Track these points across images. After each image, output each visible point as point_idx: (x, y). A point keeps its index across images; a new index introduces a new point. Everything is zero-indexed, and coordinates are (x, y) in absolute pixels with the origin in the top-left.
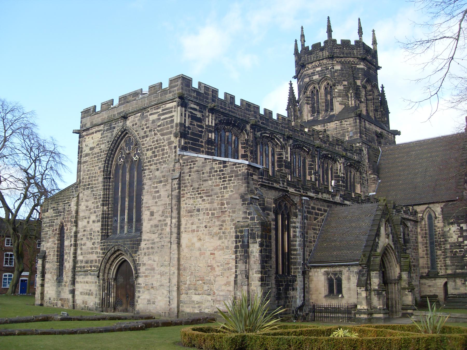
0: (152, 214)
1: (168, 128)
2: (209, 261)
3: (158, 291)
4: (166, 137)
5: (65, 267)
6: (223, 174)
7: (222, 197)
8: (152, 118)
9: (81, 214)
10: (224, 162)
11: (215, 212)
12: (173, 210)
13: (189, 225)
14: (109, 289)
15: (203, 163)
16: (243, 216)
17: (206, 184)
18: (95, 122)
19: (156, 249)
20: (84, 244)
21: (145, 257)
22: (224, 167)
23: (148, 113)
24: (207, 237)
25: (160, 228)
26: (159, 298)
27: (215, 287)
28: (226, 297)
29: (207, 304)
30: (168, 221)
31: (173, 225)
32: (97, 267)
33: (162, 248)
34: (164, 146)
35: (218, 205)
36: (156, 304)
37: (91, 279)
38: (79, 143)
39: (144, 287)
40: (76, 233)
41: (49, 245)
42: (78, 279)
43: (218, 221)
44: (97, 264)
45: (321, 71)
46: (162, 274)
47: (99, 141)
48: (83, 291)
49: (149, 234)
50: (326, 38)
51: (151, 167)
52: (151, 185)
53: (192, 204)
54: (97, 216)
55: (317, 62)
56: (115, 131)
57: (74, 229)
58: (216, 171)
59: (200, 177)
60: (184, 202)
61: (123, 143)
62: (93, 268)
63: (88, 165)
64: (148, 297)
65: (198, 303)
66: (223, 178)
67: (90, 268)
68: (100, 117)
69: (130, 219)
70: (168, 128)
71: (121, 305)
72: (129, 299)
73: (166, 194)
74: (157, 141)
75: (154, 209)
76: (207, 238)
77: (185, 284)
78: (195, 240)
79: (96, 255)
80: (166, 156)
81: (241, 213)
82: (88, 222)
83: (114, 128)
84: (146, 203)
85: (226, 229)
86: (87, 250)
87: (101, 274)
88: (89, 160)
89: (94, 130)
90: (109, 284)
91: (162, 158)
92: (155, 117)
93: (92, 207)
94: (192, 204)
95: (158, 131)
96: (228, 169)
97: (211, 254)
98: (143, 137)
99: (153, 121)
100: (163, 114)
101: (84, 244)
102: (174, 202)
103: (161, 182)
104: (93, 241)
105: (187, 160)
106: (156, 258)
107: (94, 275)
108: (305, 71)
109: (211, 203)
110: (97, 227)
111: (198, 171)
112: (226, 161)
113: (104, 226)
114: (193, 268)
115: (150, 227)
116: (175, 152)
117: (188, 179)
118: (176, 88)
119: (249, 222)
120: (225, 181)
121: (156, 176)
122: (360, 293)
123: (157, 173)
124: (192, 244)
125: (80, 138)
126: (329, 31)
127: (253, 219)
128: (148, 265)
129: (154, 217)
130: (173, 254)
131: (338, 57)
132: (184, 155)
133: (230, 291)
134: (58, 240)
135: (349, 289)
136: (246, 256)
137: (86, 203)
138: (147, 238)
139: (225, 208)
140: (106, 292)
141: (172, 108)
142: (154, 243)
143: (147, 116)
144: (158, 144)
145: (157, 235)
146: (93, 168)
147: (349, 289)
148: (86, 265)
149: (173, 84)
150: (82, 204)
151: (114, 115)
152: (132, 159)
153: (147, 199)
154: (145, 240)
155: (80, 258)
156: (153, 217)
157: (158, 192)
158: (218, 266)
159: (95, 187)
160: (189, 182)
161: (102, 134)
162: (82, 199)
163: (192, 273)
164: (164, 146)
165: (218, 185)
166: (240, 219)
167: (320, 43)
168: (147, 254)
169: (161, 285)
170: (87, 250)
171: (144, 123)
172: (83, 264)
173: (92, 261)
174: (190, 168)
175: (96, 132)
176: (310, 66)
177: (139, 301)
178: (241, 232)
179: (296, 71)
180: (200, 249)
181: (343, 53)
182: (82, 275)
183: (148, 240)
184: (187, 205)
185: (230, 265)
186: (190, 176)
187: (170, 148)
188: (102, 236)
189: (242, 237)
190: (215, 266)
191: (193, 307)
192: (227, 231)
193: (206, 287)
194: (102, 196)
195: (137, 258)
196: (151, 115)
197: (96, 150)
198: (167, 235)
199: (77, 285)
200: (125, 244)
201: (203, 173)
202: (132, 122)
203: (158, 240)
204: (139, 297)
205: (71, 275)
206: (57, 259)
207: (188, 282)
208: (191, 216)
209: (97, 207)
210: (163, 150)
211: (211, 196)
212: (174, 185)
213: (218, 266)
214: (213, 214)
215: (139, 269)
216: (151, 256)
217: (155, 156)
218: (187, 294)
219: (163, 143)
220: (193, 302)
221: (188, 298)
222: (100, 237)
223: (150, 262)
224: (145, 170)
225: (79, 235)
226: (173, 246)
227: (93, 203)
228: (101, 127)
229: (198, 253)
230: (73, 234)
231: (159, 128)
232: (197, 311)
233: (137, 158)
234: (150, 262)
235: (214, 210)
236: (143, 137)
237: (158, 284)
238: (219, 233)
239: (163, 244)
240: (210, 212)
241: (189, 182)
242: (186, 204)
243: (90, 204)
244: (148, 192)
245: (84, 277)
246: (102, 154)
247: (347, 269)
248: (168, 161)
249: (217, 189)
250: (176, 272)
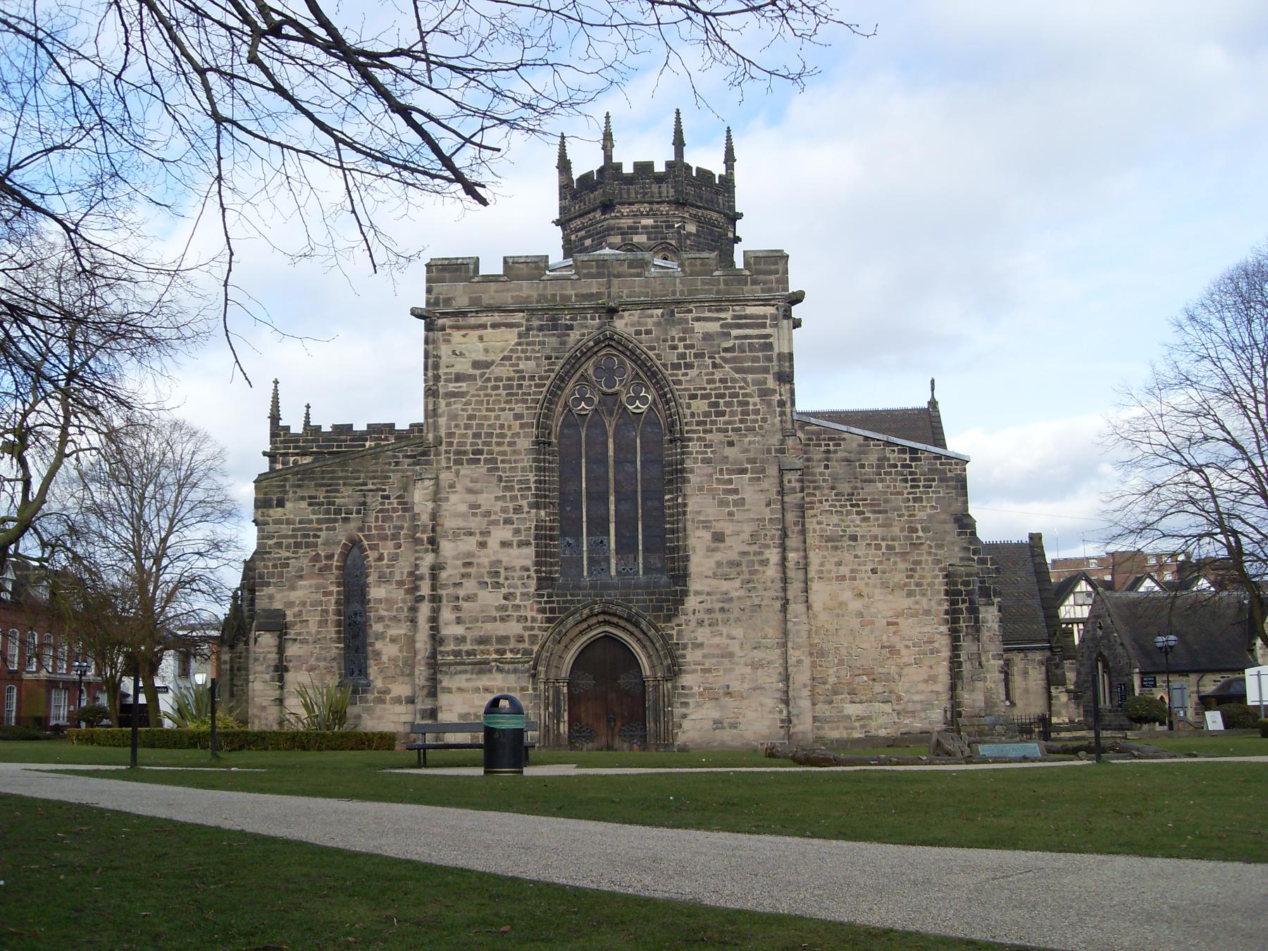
0: (719, 537)
1: (755, 359)
2: (885, 637)
3: (745, 702)
4: (750, 377)
5: (378, 654)
6: (911, 473)
7: (910, 516)
8: (700, 327)
9: (449, 523)
10: (914, 451)
11: (896, 543)
12: (790, 534)
13: (828, 567)
14: (557, 706)
15: (859, 445)
16: (961, 555)
17: (869, 488)
18: (486, 300)
19: (736, 613)
20: (468, 598)
21: (700, 630)
22: (912, 459)
23: (690, 316)
24: (877, 591)
25: (744, 568)
26: (750, 715)
27: (900, 688)
28: (928, 705)
29: (881, 720)
30: (773, 556)
31: (790, 565)
32: (527, 652)
33: (752, 611)
34: (750, 395)
35: (902, 530)
36: (742, 727)
37: (504, 680)
38: (427, 342)
39: (701, 694)
40: (436, 569)
41: (295, 595)
42: (446, 682)
43: (905, 561)
44: (526, 645)
45: (653, 227)
46: (756, 666)
47: (511, 351)
48: (472, 711)
49: (714, 582)
50: (671, 157)
51: (708, 436)
52: (711, 475)
53: (835, 525)
54: (517, 531)
56: (574, 336)
57: (429, 559)
58: (896, 466)
59: (855, 473)
60: (814, 520)
61: (589, 367)
62: (509, 655)
63: (467, 403)
64: (716, 715)
65: (859, 718)
66: (912, 480)
67: (495, 656)
68: (508, 290)
69: (626, 546)
70: (755, 359)
71: (591, 737)
72: (619, 724)
73: (762, 498)
74: (722, 381)
75: (728, 528)
76: (878, 593)
77: (824, 683)
78: (847, 595)
79: (521, 625)
80: (752, 417)
81: (957, 549)
82: (483, 545)
83: (571, 328)
84: (699, 513)
85: (922, 577)
86: (482, 611)
87: (541, 669)
88: (474, 392)
89: (484, 319)
90: (557, 692)
91: (741, 421)
92: (714, 327)
93: (497, 509)
94: (835, 525)
95: (725, 360)
96: (924, 465)
97: (889, 624)
98: (676, 367)
99: (707, 337)
100: (739, 326)
101: (468, 598)
102: (791, 517)
103: (744, 471)
104: (504, 591)
105: (818, 434)
106: (738, 632)
107: (515, 671)
108: (612, 218)
109: (886, 525)
110: (526, 557)
111: (848, 460)
112: (917, 450)
113: (542, 557)
114: (843, 652)
115: (713, 565)
116: (782, 414)
117: (821, 474)
118: (773, 277)
119: (976, 567)
120: (918, 487)
121: (727, 457)
122: (1057, 697)
123: (728, 451)
124: (841, 604)
125: (429, 328)
126: (679, 143)
127: (982, 561)
128: (712, 645)
129: (728, 543)
130: (795, 623)
131: (693, 205)
132: (810, 424)
133: (938, 693)
134: (339, 585)
135: (1027, 691)
136: (976, 628)
137: (471, 498)
138: (706, 589)
139: (918, 537)
140: (551, 709)
141: (765, 317)
142: (730, 600)
143: (686, 321)
144: (726, 388)
145: (737, 583)
146: (493, 414)
147: (1027, 691)
148: (482, 647)
149: (762, 267)
150: (453, 498)
151: (566, 298)
152: (625, 409)
153: (699, 502)
154: (697, 593)
155: (451, 630)
156: (721, 545)
157: (736, 491)
158: (907, 647)
159: (503, 461)
160: (824, 480)
161: (520, 336)
162: (452, 486)
163: (841, 662)
164: (745, 395)
165: (901, 493)
166: (956, 561)
167: (651, 165)
168: (706, 622)
169: (755, 689)
170: (482, 611)
171: (675, 332)
172: (465, 647)
173: (503, 639)
174: (828, 452)
175: (494, 326)
176: (625, 210)
177: (686, 724)
178: (966, 584)
179: (563, 210)
180: (860, 615)
181: (701, 198)
182: (466, 672)
183: (708, 594)
184: (824, 526)
185: (936, 645)
186: (826, 467)
187: (769, 404)
188: (539, 579)
189: (969, 593)
190: (899, 646)
191: (846, 728)
192: (925, 582)
193: (878, 688)
194: (533, 486)
195: (674, 632)
196: (698, 319)
197: (497, 371)
198: (769, 584)
199: (443, 699)
200: (630, 601)
201: (862, 466)
202: (633, 325)
203: (741, 593)
204: (685, 716)
205: (425, 674)
206: (338, 632)
207: (832, 680)
208: (836, 548)
209: (518, 510)
210: (747, 403)
211: (886, 512)
212: (790, 481)
213: (907, 647)
214: (889, 547)
215: (684, 656)
216: (719, 628)
217: (723, 414)
218: (831, 702)
219: (741, 388)
220: (849, 717)
221: (834, 711)
222: (533, 584)
223: (716, 640)
224: (690, 440)
225: (443, 575)
226: (792, 607)
227: (497, 498)
228: (519, 317)
229: (855, 622)
230: (424, 570)
231: (728, 355)
232: (857, 735)
233: (638, 407)
234: (716, 640)
235: (893, 540)
236: (676, 367)
237: (746, 686)
238: (906, 585)
239: (757, 601)
240: (884, 544)
241: (824, 480)
242: (819, 523)
243: (486, 500)
244: (701, 489)
245: (474, 676)
246: (526, 383)
247: (1022, 655)
248: (761, 428)
249: (898, 501)
250: (807, 661)
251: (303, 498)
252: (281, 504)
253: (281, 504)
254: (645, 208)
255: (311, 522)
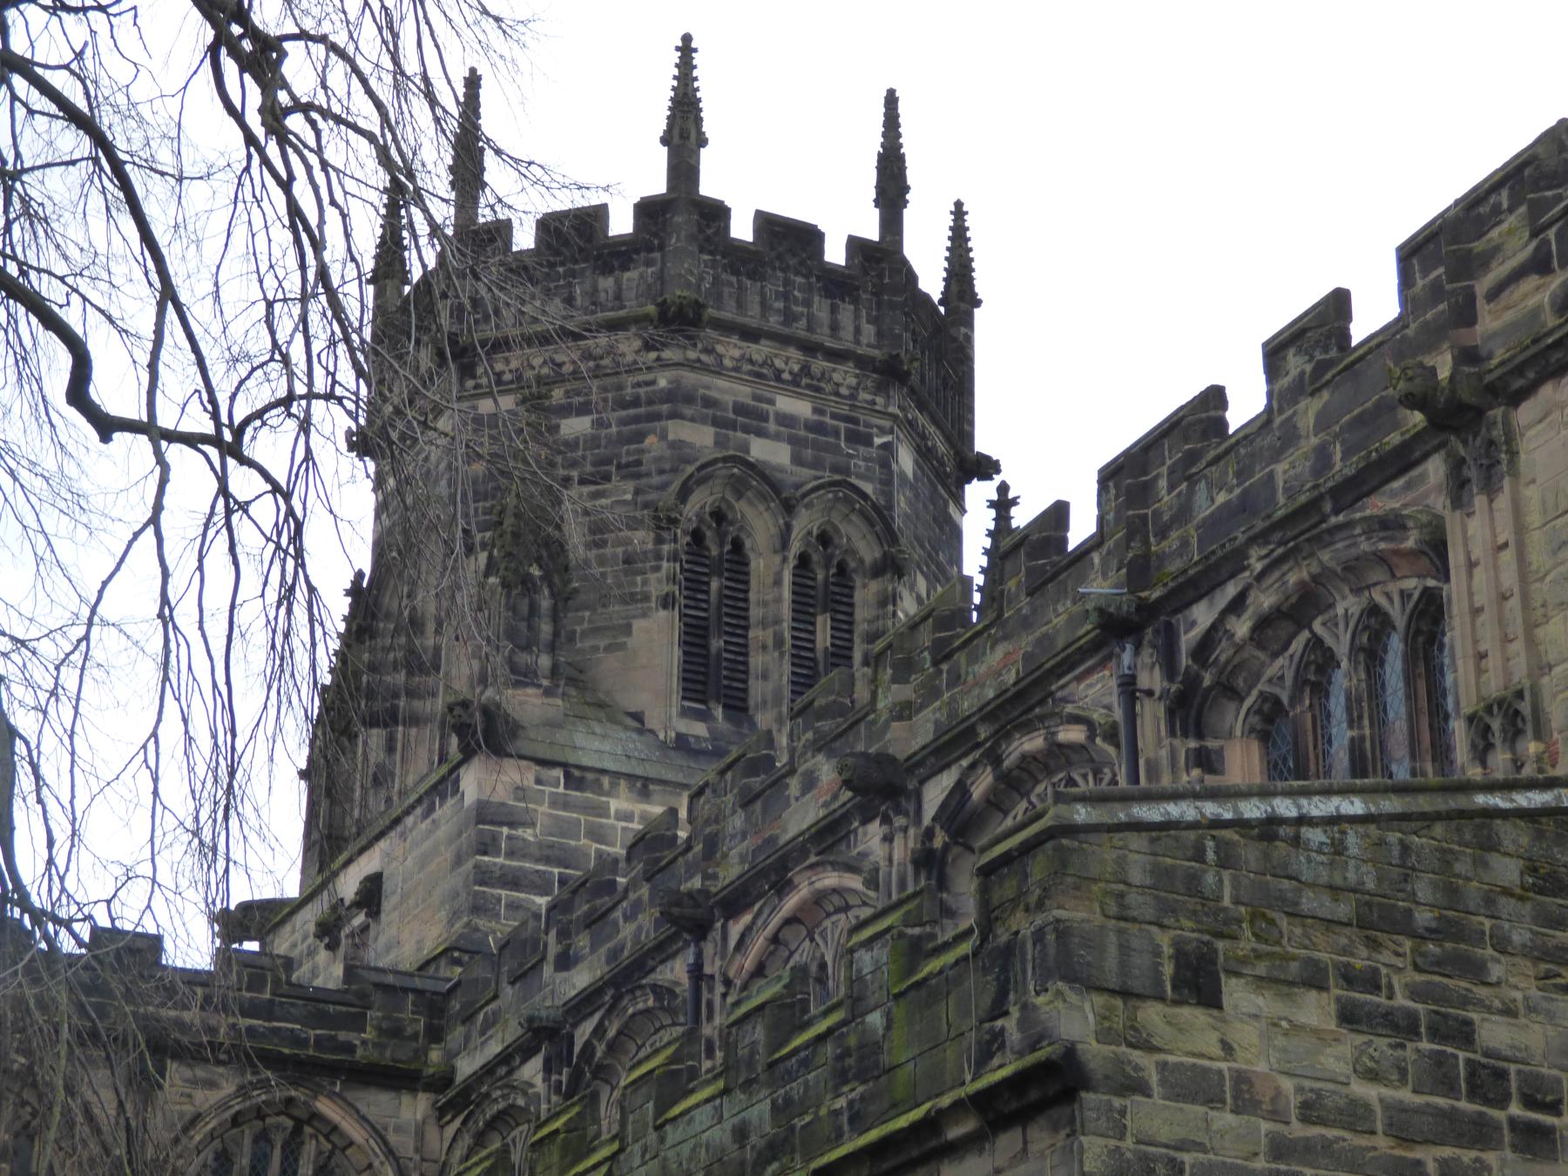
55: (793, 353)
176: (731, 349)
251: (1314, 979)
252: (1199, 982)
253: (1199, 982)
254: (790, 360)
255: (1355, 1116)
